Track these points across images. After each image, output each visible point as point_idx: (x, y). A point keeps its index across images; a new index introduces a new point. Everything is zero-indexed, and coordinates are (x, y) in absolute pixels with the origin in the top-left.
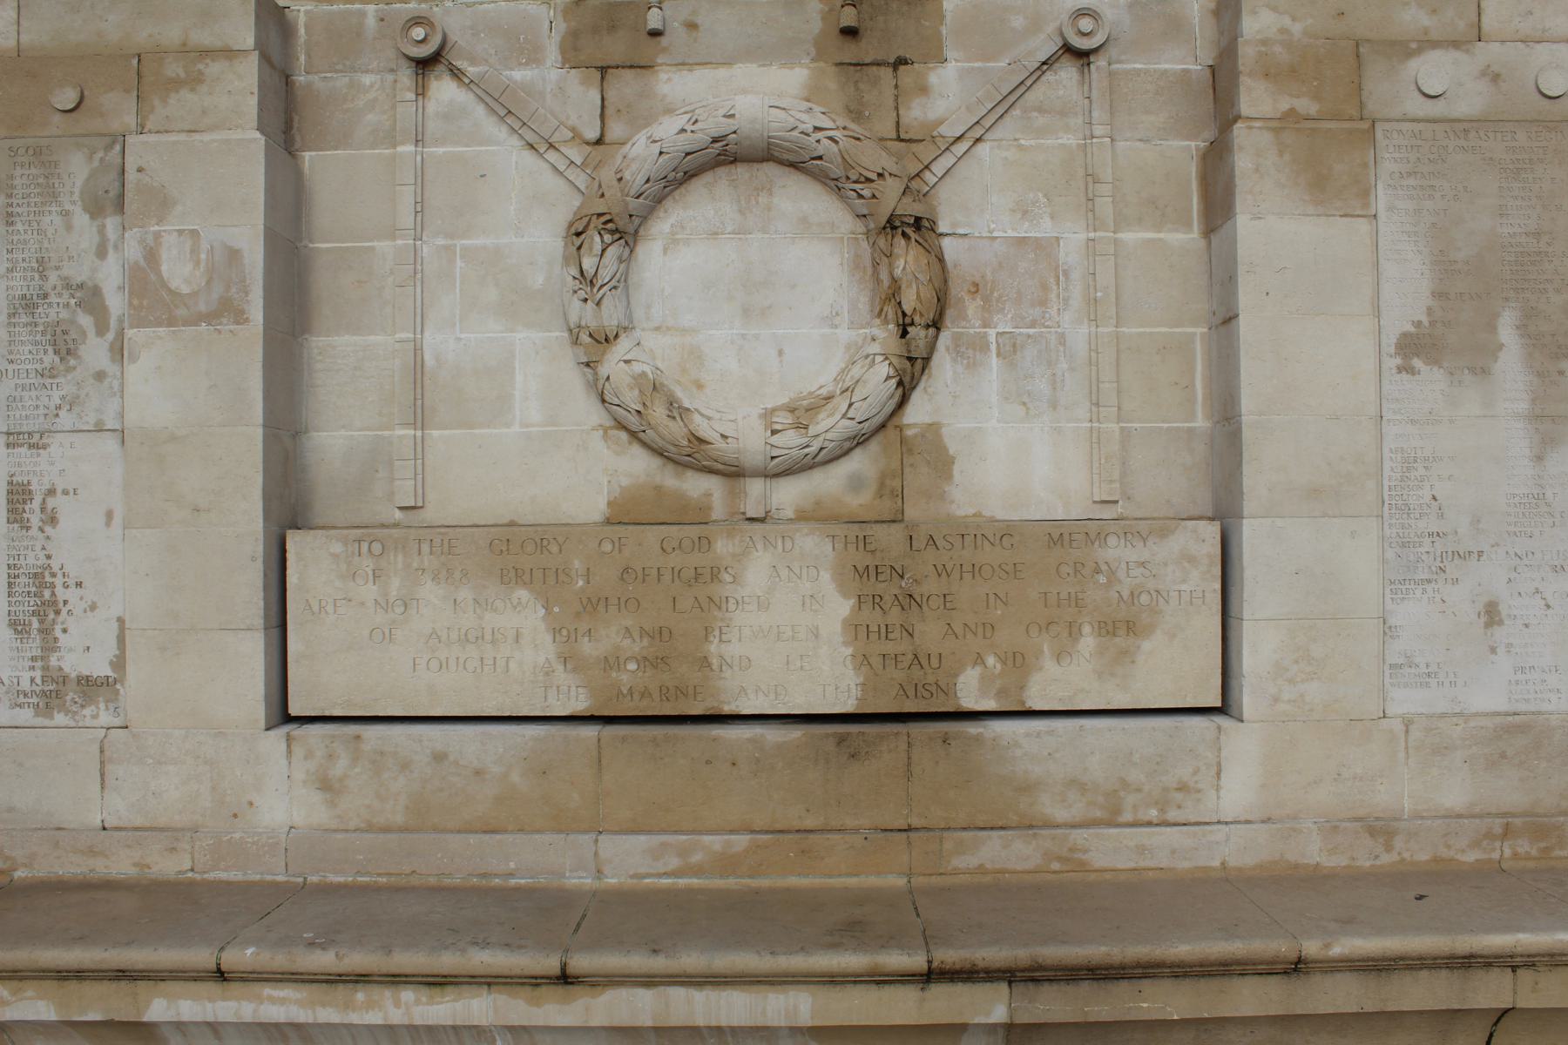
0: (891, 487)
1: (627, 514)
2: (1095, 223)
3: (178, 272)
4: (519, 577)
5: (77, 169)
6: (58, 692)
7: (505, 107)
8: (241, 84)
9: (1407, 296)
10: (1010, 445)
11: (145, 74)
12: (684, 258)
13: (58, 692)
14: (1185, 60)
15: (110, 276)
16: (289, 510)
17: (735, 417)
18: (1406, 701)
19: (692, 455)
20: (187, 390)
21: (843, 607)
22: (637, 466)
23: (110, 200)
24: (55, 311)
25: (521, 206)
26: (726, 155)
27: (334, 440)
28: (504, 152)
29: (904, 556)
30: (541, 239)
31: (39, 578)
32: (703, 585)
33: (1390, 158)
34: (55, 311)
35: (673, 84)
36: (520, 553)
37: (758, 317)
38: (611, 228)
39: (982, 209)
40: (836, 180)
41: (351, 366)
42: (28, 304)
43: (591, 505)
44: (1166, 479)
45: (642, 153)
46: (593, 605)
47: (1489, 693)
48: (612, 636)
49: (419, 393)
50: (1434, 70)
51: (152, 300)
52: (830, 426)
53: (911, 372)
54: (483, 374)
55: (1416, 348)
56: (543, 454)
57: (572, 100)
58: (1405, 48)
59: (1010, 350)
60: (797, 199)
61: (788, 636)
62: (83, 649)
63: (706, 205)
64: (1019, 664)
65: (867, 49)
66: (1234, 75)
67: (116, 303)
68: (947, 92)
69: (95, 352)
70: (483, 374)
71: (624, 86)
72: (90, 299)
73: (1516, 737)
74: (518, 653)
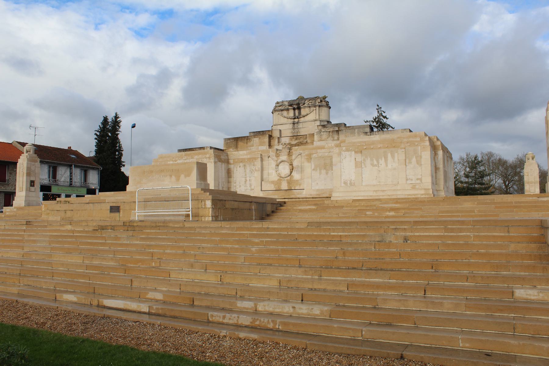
0: (291, 178)
3: (257, 169)
5: (252, 164)
6: (252, 190)
8: (259, 159)
9: (313, 167)
11: (255, 159)
12: (281, 167)
13: (252, 190)
16: (262, 180)
17: (283, 175)
19: (281, 177)
20: (257, 174)
23: (254, 165)
25: (273, 164)
26: (282, 161)
27: (265, 176)
28: (272, 161)
30: (274, 166)
32: (280, 183)
35: (281, 157)
36: (273, 182)
38: (278, 165)
39: (295, 164)
41: (265, 172)
43: (276, 180)
45: (280, 160)
47: (317, 188)
48: (277, 186)
49: (269, 174)
50: (314, 155)
51: (256, 170)
52: (287, 175)
53: (291, 172)
54: (272, 174)
55: (313, 170)
56: (274, 177)
57: (276, 159)
58: (313, 154)
60: (286, 163)
61: (284, 186)
62: (253, 187)
63: (282, 164)
68: (294, 157)
70: (272, 174)
73: (318, 190)
74: (272, 187)
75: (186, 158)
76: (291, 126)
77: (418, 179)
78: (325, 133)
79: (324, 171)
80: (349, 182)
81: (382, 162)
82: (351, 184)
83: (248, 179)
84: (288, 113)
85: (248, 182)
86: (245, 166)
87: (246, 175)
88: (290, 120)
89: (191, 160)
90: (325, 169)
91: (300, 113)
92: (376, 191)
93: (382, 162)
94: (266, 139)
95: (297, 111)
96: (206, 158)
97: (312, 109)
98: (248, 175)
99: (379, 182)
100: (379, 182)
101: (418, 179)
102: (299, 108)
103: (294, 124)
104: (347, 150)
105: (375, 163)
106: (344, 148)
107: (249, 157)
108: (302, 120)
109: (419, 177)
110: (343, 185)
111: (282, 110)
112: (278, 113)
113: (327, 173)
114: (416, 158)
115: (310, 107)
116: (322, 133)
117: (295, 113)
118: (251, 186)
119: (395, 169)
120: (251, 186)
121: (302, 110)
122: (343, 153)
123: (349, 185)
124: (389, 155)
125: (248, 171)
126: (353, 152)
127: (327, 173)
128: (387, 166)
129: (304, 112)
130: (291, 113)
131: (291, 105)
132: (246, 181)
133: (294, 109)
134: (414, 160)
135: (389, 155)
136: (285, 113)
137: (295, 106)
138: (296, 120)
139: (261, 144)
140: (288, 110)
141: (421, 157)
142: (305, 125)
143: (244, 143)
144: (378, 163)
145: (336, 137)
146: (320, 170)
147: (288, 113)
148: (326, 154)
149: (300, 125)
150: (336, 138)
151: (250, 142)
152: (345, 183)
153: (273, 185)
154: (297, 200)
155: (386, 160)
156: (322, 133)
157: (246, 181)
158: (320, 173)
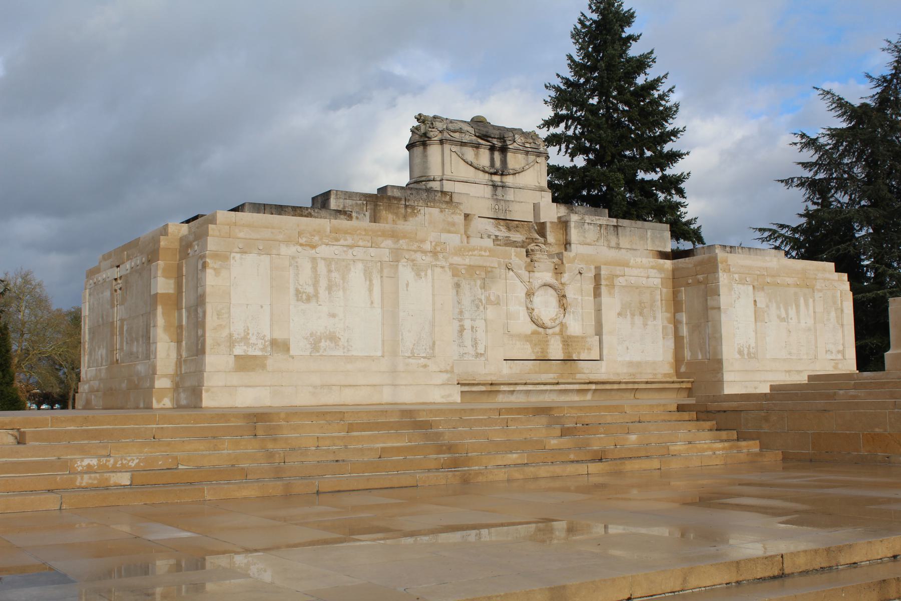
0: (561, 331)
1: (534, 333)
2: (582, 295)
3: (492, 298)
4: (527, 341)
6: (478, 355)
7: (518, 276)
9: (618, 310)
10: (575, 327)
12: (537, 300)
13: (478, 355)
14: (592, 274)
15: (483, 298)
18: (619, 359)
21: (561, 346)
22: (534, 327)
24: (477, 302)
28: (518, 282)
29: (567, 341)
30: (523, 295)
31: (475, 339)
33: (617, 290)
34: (477, 302)
35: (537, 274)
37: (546, 306)
39: (571, 293)
40: (555, 290)
42: (473, 301)
43: (529, 332)
44: (591, 330)
46: (535, 345)
47: (628, 359)
48: (537, 349)
50: (621, 279)
55: (619, 314)
58: (617, 276)
59: (573, 313)
61: (556, 350)
62: (481, 350)
64: (579, 353)
65: (558, 271)
66: (600, 278)
67: (484, 302)
68: (566, 277)
69: (481, 308)
71: (532, 274)
72: (481, 301)
73: (631, 364)
75: (350, 241)
76: (488, 190)
77: (839, 352)
78: (591, 227)
79: (638, 320)
80: (746, 352)
81: (792, 312)
82: (749, 354)
83: (467, 324)
84: (477, 155)
85: (467, 334)
86: (458, 286)
87: (461, 313)
88: (481, 174)
89: (373, 251)
90: (641, 314)
91: (504, 162)
92: (789, 371)
93: (792, 312)
94: (459, 219)
95: (497, 155)
96: (424, 252)
97: (531, 158)
98: (467, 315)
99: (790, 354)
100: (790, 354)
101: (839, 352)
102: (504, 150)
103: (495, 186)
104: (742, 282)
105: (783, 315)
106: (736, 276)
107: (467, 261)
108: (509, 180)
109: (841, 348)
110: (737, 356)
111: (463, 144)
112: (454, 148)
113: (645, 325)
114: (836, 310)
115: (527, 153)
116: (586, 226)
117: (492, 160)
118: (475, 344)
119: (809, 330)
120: (475, 344)
121: (510, 156)
122: (735, 286)
123: (746, 357)
124: (802, 301)
125: (467, 300)
126: (751, 288)
127: (645, 325)
128: (799, 322)
129: (514, 160)
130: (484, 158)
131: (485, 137)
132: (462, 330)
133: (492, 149)
134: (833, 314)
135: (802, 301)
136: (469, 153)
137: (495, 141)
138: (497, 178)
139: (450, 228)
140: (477, 146)
141: (842, 311)
142: (521, 195)
143: (397, 214)
144: (787, 317)
145: (613, 241)
146: (633, 315)
147: (477, 155)
148: (644, 281)
149: (510, 195)
150: (613, 244)
151: (414, 214)
152: (740, 352)
153: (528, 346)
154: (616, 386)
155: (798, 311)
156: (586, 226)
157: (462, 330)
158: (633, 324)
